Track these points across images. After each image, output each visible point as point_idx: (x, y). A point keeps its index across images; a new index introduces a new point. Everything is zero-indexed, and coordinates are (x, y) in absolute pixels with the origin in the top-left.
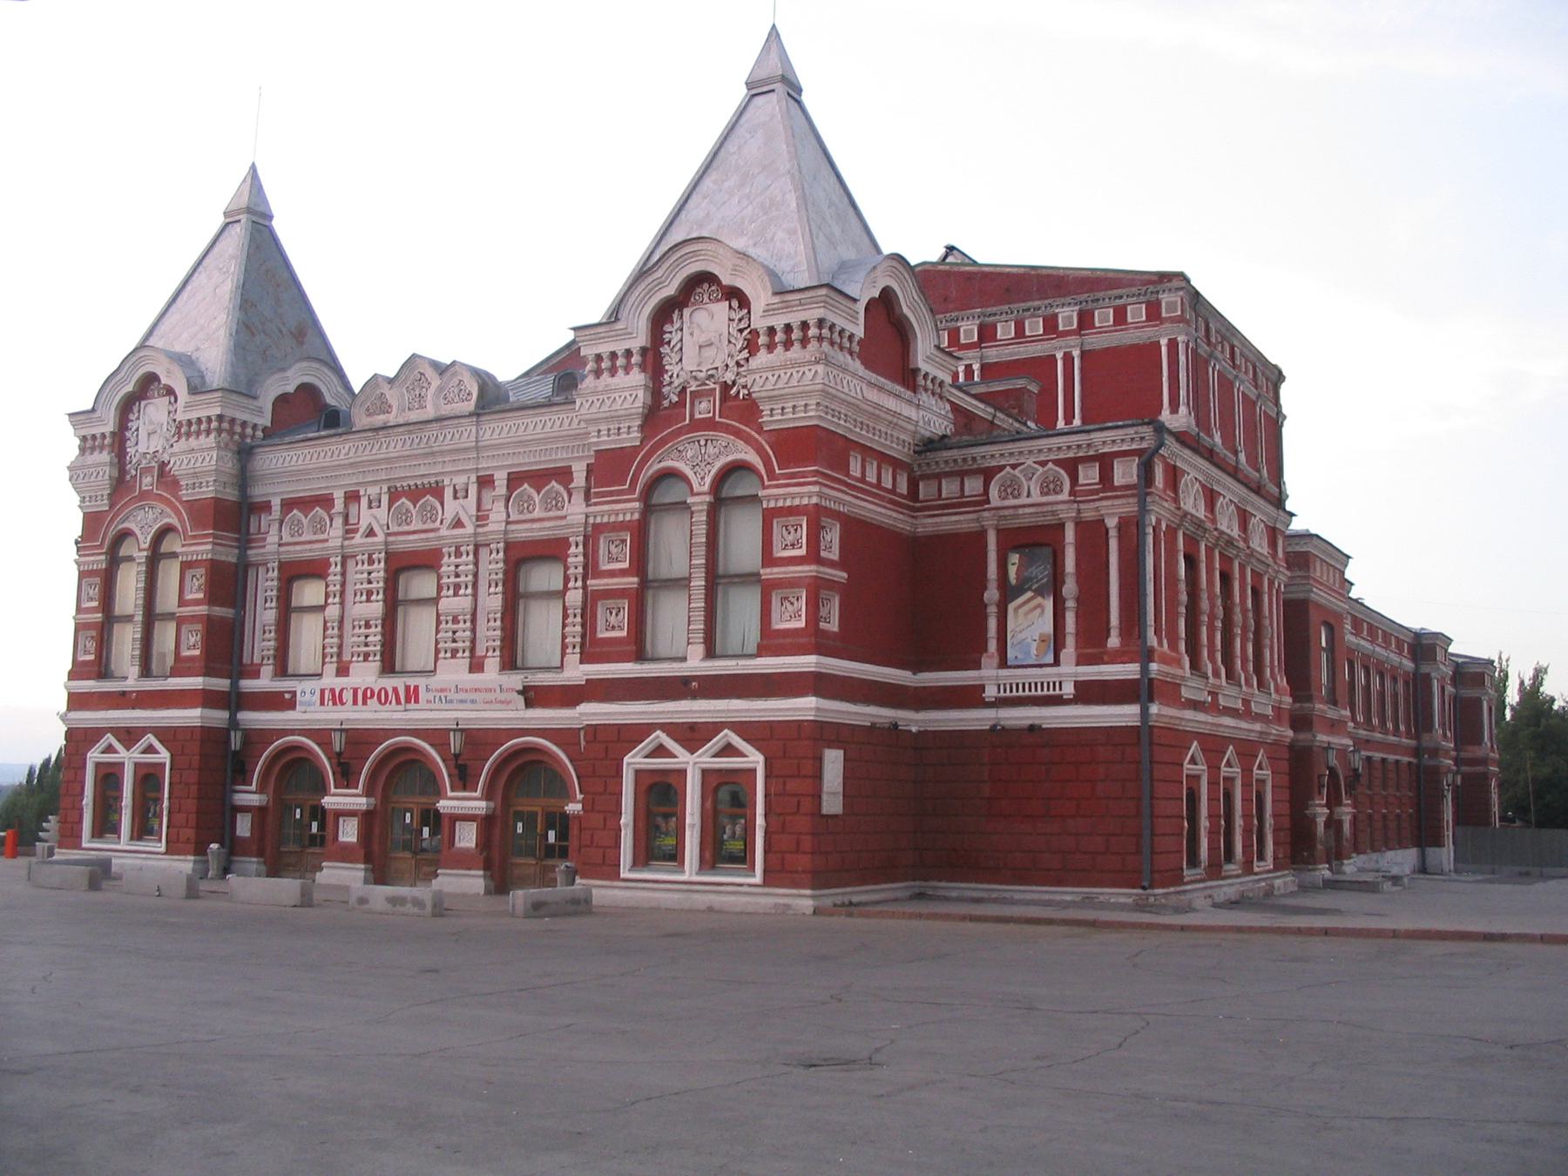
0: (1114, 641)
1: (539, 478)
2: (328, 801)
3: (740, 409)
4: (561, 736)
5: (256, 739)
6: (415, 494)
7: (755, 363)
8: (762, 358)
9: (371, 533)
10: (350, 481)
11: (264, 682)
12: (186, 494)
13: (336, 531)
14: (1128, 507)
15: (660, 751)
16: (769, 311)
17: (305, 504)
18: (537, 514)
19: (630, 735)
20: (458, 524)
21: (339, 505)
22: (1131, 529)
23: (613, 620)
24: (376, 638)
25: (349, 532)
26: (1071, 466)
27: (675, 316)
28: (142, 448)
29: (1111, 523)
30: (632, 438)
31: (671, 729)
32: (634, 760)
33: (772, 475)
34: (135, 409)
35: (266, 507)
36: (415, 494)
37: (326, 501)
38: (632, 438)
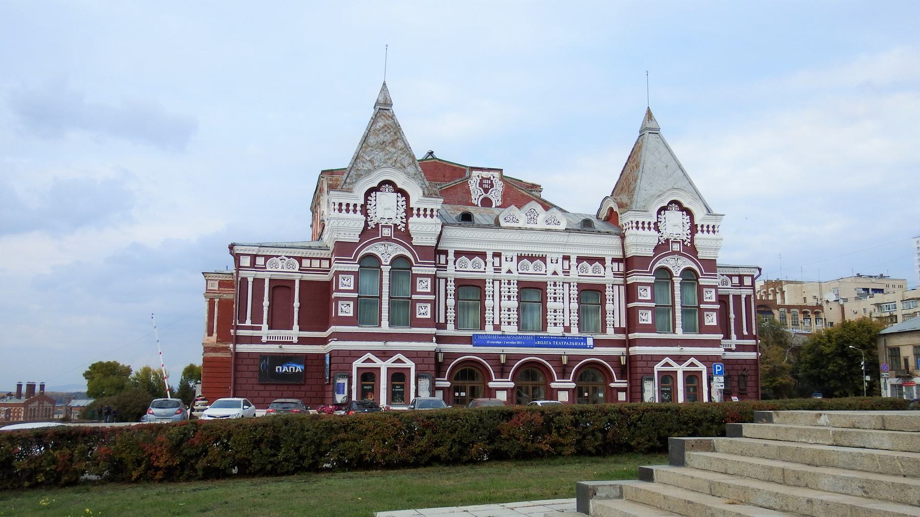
0: (745, 333)
1: (591, 260)
2: (553, 385)
3: (691, 250)
4: (615, 360)
5: (450, 356)
6: (532, 258)
7: (697, 236)
8: (698, 235)
9: (509, 271)
10: (498, 248)
11: (450, 330)
12: (415, 242)
13: (490, 268)
14: (750, 292)
15: (667, 364)
16: (703, 219)
17: (471, 255)
18: (590, 273)
19: (658, 358)
20: (555, 273)
21: (489, 258)
22: (748, 298)
23: (643, 317)
24: (514, 315)
25: (497, 270)
26: (730, 276)
27: (663, 212)
28: (379, 215)
29: (744, 296)
30: (651, 254)
31: (671, 357)
32: (658, 367)
33: (702, 274)
34: (373, 194)
35: (446, 253)
36: (532, 258)
37: (483, 255)
38: (651, 254)
